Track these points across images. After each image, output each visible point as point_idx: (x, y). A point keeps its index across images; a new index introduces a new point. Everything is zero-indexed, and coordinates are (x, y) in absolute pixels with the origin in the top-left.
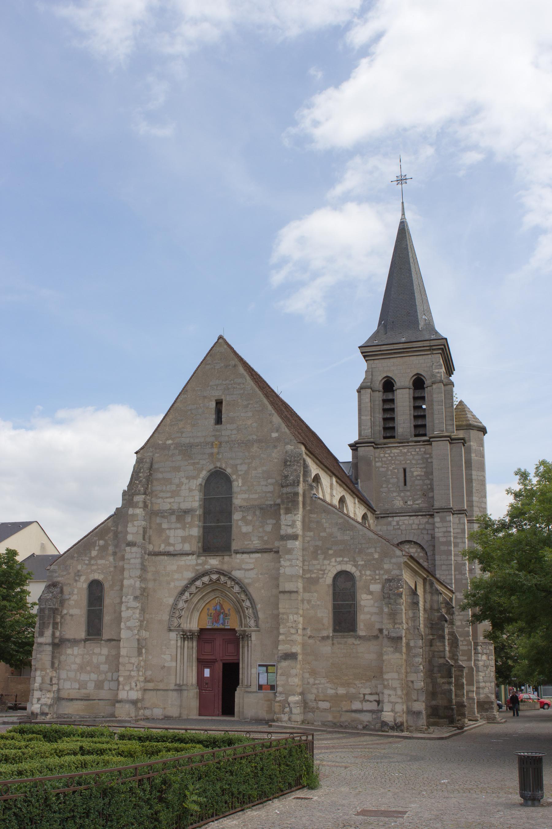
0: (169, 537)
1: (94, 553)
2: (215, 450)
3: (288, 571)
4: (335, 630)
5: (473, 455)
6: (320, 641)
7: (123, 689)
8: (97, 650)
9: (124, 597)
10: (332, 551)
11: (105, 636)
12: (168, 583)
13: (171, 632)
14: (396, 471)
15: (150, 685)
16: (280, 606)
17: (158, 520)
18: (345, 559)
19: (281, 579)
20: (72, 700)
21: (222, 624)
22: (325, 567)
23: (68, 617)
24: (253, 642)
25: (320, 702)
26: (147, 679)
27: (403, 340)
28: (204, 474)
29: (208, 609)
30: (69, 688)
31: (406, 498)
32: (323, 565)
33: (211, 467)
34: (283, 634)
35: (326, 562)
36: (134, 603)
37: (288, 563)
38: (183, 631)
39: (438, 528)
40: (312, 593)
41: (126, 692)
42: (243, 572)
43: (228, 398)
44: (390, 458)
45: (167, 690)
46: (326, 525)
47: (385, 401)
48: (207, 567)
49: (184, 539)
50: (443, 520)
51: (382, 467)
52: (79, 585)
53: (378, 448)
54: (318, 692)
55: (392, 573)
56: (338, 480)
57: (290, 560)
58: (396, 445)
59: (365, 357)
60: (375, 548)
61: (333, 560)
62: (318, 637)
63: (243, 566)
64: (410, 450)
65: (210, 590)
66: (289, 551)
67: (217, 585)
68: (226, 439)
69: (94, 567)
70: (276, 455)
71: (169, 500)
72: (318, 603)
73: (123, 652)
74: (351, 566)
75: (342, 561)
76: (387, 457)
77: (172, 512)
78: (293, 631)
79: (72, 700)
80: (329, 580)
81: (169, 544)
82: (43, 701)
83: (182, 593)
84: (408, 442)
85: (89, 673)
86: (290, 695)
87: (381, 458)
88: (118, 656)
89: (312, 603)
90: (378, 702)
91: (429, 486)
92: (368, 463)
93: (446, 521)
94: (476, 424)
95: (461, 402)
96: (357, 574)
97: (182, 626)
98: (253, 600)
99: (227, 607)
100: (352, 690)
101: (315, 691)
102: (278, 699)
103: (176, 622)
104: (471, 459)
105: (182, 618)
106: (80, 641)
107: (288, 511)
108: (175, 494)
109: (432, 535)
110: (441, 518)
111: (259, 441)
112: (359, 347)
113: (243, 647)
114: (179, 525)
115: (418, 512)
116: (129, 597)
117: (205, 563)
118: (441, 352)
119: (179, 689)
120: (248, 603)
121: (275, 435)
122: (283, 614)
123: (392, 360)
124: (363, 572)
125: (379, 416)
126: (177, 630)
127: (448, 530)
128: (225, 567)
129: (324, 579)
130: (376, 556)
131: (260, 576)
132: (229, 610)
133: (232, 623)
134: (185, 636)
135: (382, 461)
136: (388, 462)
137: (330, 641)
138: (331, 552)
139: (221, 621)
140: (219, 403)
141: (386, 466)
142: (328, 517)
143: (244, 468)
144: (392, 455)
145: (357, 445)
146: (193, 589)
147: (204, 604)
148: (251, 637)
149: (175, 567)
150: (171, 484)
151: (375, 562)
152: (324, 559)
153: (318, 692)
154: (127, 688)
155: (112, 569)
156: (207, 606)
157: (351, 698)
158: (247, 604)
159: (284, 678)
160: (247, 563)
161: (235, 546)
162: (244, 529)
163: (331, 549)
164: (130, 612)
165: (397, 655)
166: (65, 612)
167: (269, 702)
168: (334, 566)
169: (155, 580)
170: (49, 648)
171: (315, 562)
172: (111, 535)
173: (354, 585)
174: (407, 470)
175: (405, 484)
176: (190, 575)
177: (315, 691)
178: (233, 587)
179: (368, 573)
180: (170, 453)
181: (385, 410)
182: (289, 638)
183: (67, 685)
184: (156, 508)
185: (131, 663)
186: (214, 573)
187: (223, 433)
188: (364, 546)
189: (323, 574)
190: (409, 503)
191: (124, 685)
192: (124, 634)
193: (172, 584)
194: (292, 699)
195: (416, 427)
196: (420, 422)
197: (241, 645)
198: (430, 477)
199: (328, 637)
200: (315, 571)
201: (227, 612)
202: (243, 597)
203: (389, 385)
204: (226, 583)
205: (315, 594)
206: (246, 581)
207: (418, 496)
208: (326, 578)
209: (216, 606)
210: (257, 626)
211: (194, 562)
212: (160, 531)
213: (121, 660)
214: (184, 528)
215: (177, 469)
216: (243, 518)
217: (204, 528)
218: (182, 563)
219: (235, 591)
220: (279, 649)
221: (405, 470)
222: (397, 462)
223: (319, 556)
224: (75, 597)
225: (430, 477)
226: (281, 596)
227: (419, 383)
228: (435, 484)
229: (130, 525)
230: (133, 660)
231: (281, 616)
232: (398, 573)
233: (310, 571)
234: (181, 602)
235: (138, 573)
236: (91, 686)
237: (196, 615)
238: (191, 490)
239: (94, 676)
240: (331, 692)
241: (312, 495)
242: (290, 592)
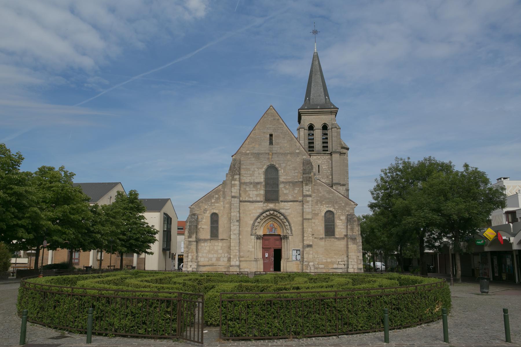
0: (249, 194)
1: (213, 201)
2: (270, 157)
3: (308, 210)
4: (325, 235)
8: (216, 244)
11: (220, 237)
17: (244, 187)
20: (205, 266)
23: (201, 229)
28: (265, 167)
30: (202, 260)
33: (269, 164)
35: (322, 207)
37: (307, 207)
43: (276, 134)
46: (321, 191)
48: (268, 208)
49: (257, 195)
52: (206, 215)
57: (308, 205)
66: (308, 202)
67: (274, 216)
68: (275, 152)
69: (213, 207)
70: (299, 159)
71: (249, 178)
73: (232, 244)
77: (251, 183)
79: (205, 266)
80: (323, 214)
81: (250, 197)
82: (193, 267)
83: (257, 219)
85: (213, 254)
90: (345, 265)
96: (335, 212)
100: (334, 260)
101: (318, 260)
102: (304, 264)
103: (254, 232)
106: (208, 240)
107: (307, 184)
108: (252, 175)
111: (291, 154)
113: (284, 242)
114: (254, 189)
117: (268, 206)
119: (256, 260)
120: (287, 224)
121: (297, 151)
128: (277, 208)
130: (343, 205)
137: (324, 240)
138: (324, 202)
140: (271, 135)
143: (284, 165)
146: (262, 217)
149: (253, 208)
150: (250, 170)
155: (222, 208)
157: (332, 263)
161: (281, 199)
162: (285, 192)
164: (235, 227)
165: (355, 246)
166: (199, 227)
170: (195, 243)
171: (317, 207)
172: (221, 193)
173: (334, 216)
176: (261, 211)
177: (318, 260)
180: (249, 157)
183: (202, 259)
184: (243, 181)
187: (274, 149)
192: (232, 237)
193: (252, 215)
194: (311, 264)
195: (323, 147)
196: (325, 145)
199: (322, 238)
202: (285, 221)
203: (311, 127)
206: (287, 214)
212: (246, 191)
214: (257, 190)
215: (253, 164)
216: (284, 187)
217: (266, 191)
218: (257, 206)
224: (204, 220)
229: (233, 188)
236: (214, 260)
237: (262, 228)
238: (259, 174)
239: (215, 256)
240: (325, 261)
242: (309, 219)
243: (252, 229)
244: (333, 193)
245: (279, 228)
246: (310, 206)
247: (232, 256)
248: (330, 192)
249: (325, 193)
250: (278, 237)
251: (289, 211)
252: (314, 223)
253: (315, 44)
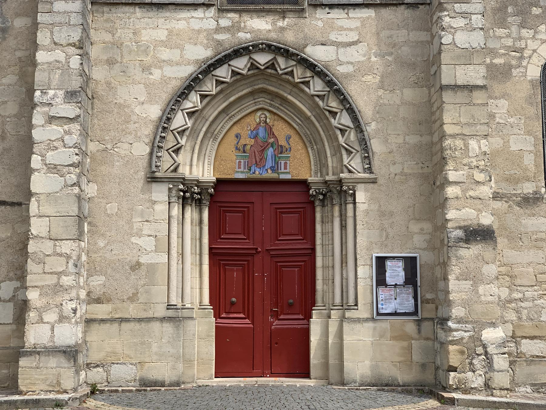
3: (462, 39)
6: (519, 204)
7: (41, 321)
9: (38, 93)
10: (540, 10)
12: (146, 69)
13: (154, 185)
15: (101, 311)
16: (447, 118)
19: (445, 58)
21: (272, 168)
24: (361, 207)
25: (524, 341)
26: (93, 296)
29: (237, 136)
32: (520, 38)
34: (456, 183)
36: (68, 106)
37: (460, 22)
38: (183, 181)
40: (496, 98)
41: (48, 327)
42: (332, 49)
45: (149, 320)
48: (244, 37)
54: (520, 318)
57: (465, 15)
62: (515, 195)
63: (333, 37)
65: (249, 90)
72: (511, 120)
73: (37, 227)
78: (480, 177)
83: (183, 94)
86: (483, 325)
88: (24, 240)
89: (498, 120)
97: (180, 170)
98: (359, 111)
99: (281, 131)
103: (166, 162)
105: (182, 151)
116: (51, 92)
120: (345, 119)
122: (454, 136)
126: (170, 180)
128: (290, 38)
129: (522, 70)
131: (373, 59)
132: (288, 138)
133: (298, 165)
134: (188, 195)
138: (536, 11)
139: (269, 163)
147: (232, 123)
148: (354, 195)
149: (162, 35)
152: (522, 26)
153: (520, 318)
154: (51, 317)
156: (236, 130)
158: (343, 121)
159: (467, 285)
160: (342, 29)
167: (405, 344)
169: (111, 62)
171: (501, 32)
178: (307, 84)
182: (471, 193)
185: (61, 255)
186: (262, 50)
189: (522, 58)
191: (40, 311)
192: (39, 183)
193: (157, 74)
194: (492, 335)
197: (318, 216)
200: (502, 51)
201: (282, 142)
202: (334, 104)
204: (291, 73)
205: (503, 104)
206: (342, 69)
208: (526, 68)
209: (257, 128)
210: (370, 170)
211: (212, 24)
213: (32, 247)
218: (182, 25)
219: (313, 92)
220: (448, 216)
223: (510, 19)
226: (447, 96)
230: (66, 247)
231: (448, 142)
233: (493, 52)
234: (180, 114)
235: (76, 35)
242: (471, 88)
243: (156, 147)
245: (296, 144)
246: (477, 20)
247: (32, 295)
250: (294, 197)
251: (355, 54)
252: (492, 116)
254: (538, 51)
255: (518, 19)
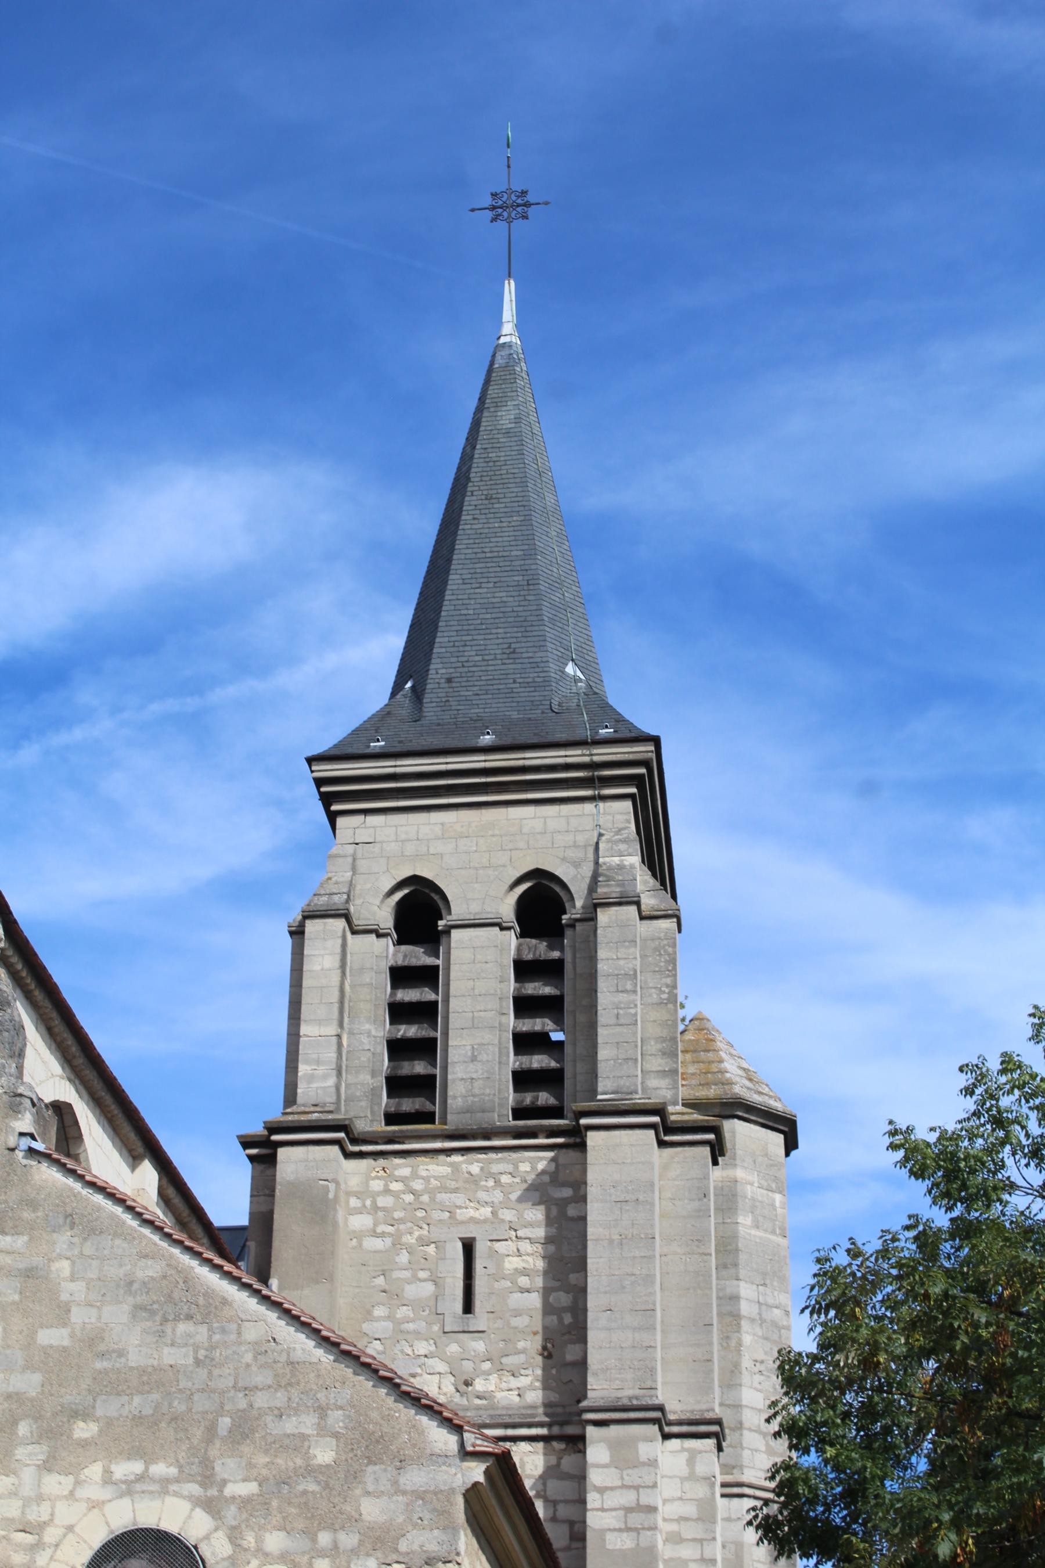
5: (745, 1220)
14: (431, 1249)
18: (159, 1469)
22: (38, 1513)
27: (487, 739)
31: (468, 1365)
32: (40, 1498)
35: (55, 1484)
39: (601, 1490)
44: (409, 1198)
46: (73, 1290)
47: (400, 976)
50: (623, 1459)
51: (374, 1234)
53: (361, 1155)
55: (403, 1546)
56: (171, 1192)
58: (438, 1145)
59: (327, 800)
60: (322, 1411)
61: (95, 1471)
64: (495, 1168)
74: (187, 1506)
75: (141, 1478)
76: (396, 1195)
84: (487, 1136)
87: (374, 1195)
91: (568, 1319)
92: (320, 1208)
93: (636, 1464)
94: (756, 1099)
95: (697, 1019)
104: (735, 1236)
109: (571, 1523)
110: (614, 1446)
112: (310, 760)
115: (514, 1426)
118: (633, 790)
123: (436, 816)
124: (249, 1540)
125: (373, 1032)
127: (645, 1500)
130: (324, 1454)
135: (376, 1208)
136: (398, 1215)
138: (84, 1430)
141: (390, 1229)
142: (88, 1249)
144: (418, 1185)
145: (275, 1137)
151: (313, 1487)
152: (47, 1466)
163: (85, 1415)
168: (95, 1505)
174: (480, 1249)
175: (468, 1307)
179: (275, 1541)
181: (398, 1012)
188: (261, 1400)
190: (479, 1385)
195: (523, 1079)
198: (573, 1278)
203: (420, 913)
207: (522, 1358)
221: (468, 1248)
222: (436, 1215)
223: (20, 1453)
225: (573, 1278)
227: (541, 906)
228: (592, 1302)
232: (433, 1547)
241: (12, 1141)
244: (209, 1310)
248: (163, 1308)
249: (116, 1316)
253: (510, 290)
254: (77, 1529)
255: (38, 1453)
